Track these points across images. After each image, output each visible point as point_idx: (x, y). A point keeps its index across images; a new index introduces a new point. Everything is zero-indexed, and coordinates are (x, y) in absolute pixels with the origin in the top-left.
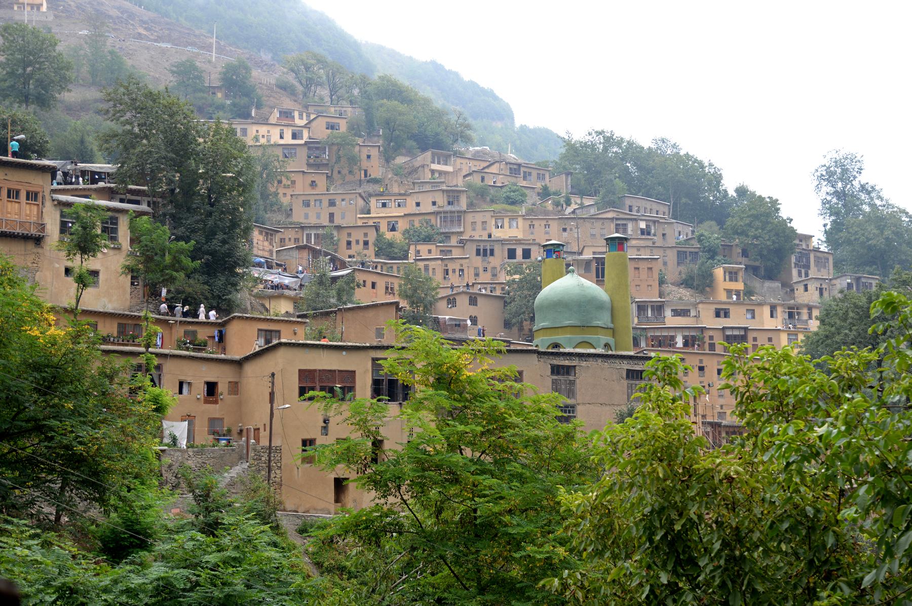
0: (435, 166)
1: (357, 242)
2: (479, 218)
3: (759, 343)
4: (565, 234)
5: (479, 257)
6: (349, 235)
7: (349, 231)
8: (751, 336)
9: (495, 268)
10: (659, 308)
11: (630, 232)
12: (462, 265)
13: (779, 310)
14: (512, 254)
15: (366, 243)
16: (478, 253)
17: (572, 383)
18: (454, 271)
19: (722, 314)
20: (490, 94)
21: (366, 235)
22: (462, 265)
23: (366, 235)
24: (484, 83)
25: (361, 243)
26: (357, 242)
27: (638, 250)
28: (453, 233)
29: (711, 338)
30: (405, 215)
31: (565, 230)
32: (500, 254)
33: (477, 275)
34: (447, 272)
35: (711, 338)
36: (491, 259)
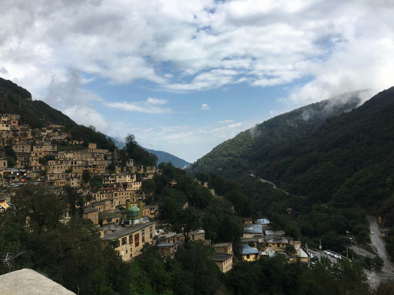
0: (42, 134)
1: (34, 159)
2: (62, 152)
3: (129, 185)
4: (82, 156)
6: (32, 158)
7: (32, 157)
8: (128, 183)
10: (108, 177)
13: (130, 176)
14: (72, 163)
15: (36, 160)
17: (144, 232)
20: (25, 90)
21: (36, 158)
23: (36, 158)
25: (35, 160)
26: (34, 159)
29: (121, 185)
33: (65, 168)
35: (121, 185)
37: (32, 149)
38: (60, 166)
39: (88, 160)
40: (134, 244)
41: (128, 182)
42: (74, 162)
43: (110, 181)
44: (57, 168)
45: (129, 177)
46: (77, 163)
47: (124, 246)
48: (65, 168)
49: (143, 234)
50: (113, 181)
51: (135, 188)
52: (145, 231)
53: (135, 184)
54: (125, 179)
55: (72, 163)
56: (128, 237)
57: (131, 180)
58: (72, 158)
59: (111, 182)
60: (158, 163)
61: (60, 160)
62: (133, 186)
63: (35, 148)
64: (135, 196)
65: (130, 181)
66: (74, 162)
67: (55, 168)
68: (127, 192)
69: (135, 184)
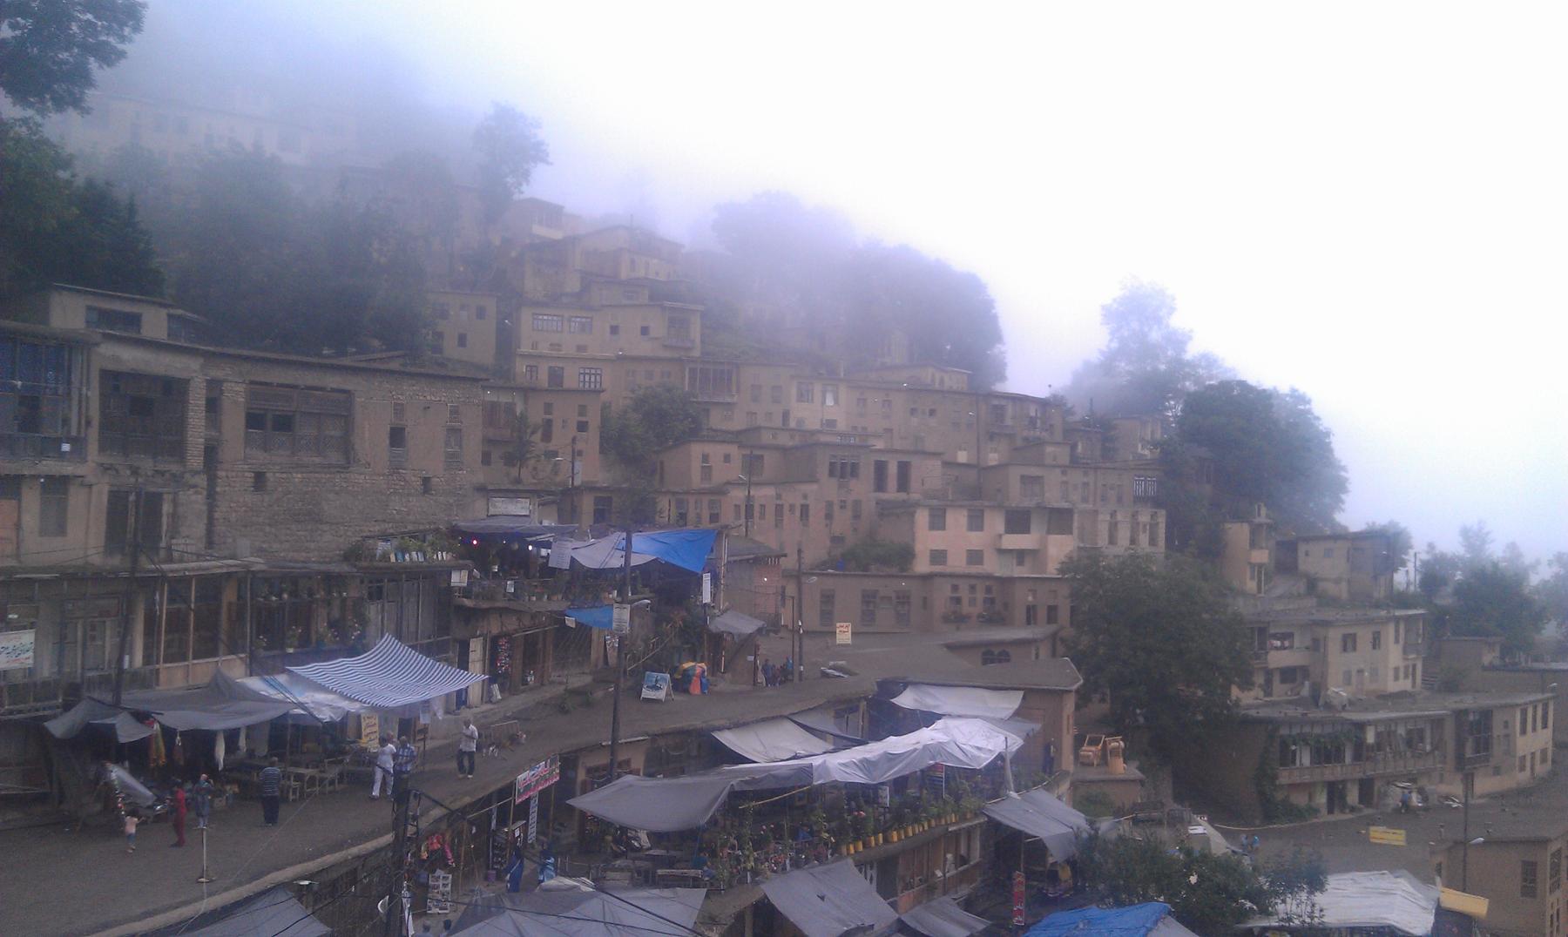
4: (915, 421)
5: (834, 482)
9: (857, 503)
11: (1009, 422)
12: (805, 497)
14: (881, 468)
15: (582, 427)
16: (831, 474)
18: (792, 508)
19: (1349, 644)
21: (582, 410)
22: (805, 497)
27: (1086, 474)
28: (718, 404)
30: (619, 358)
31: (913, 411)
32: (867, 471)
33: (829, 516)
34: (779, 509)
36: (853, 483)
38: (792, 497)
42: (893, 469)
44: (770, 510)
45: (1397, 641)
48: (829, 516)
55: (881, 468)
57: (1406, 677)
59: (1276, 679)
66: (893, 469)
67: (762, 516)
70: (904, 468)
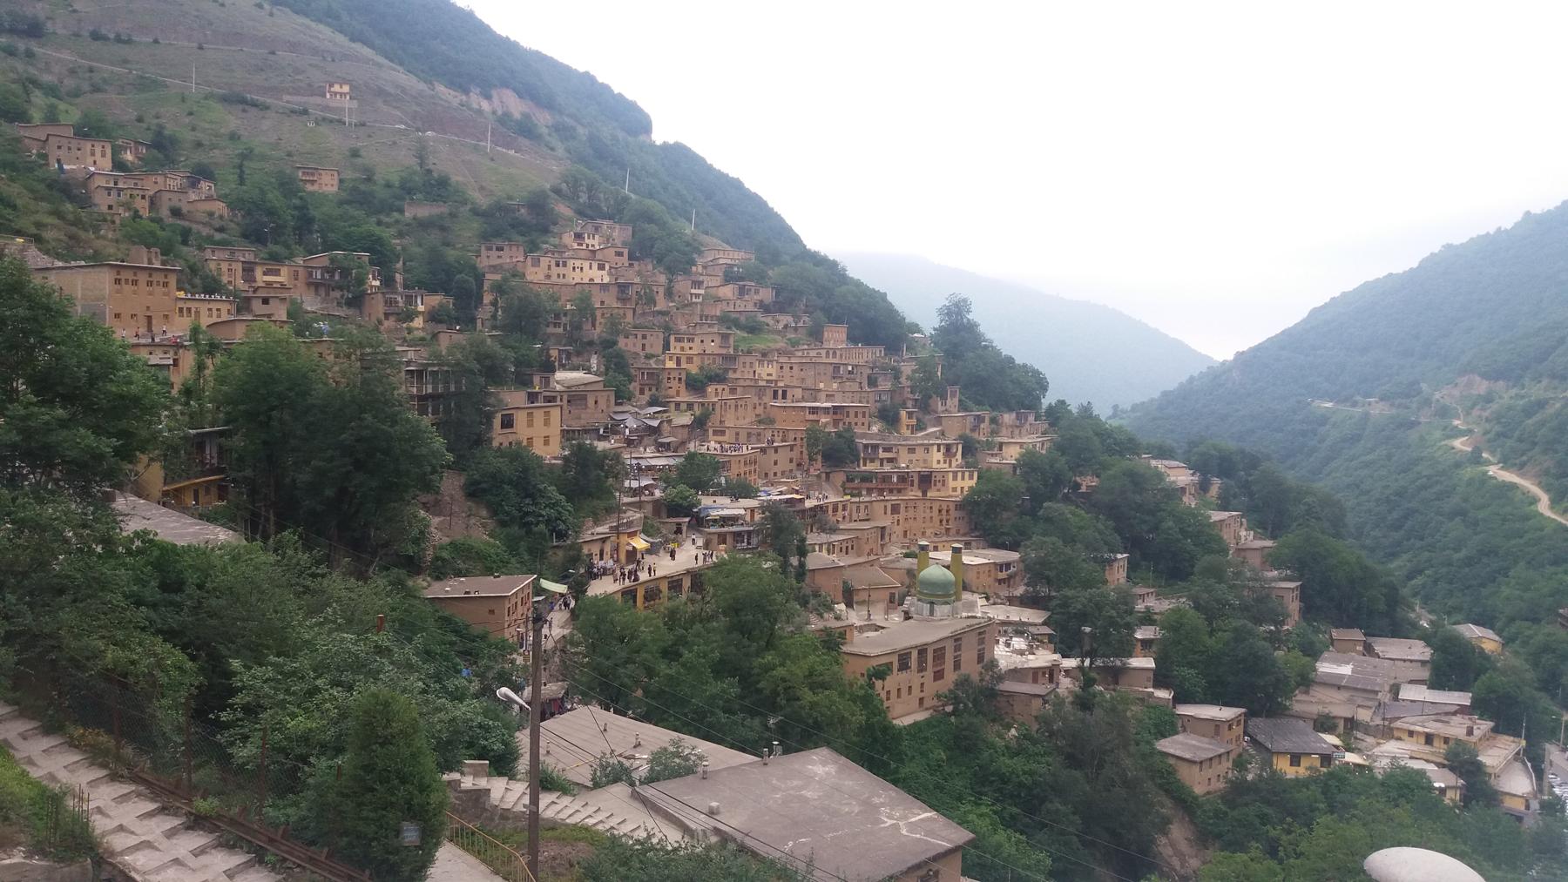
14: (775, 393)
20: (633, 107)
24: (630, 96)
32: (770, 393)
37: (666, 346)
39: (822, 386)
40: (929, 673)
41: (935, 465)
43: (882, 460)
46: (789, 395)
47: (904, 675)
49: (957, 648)
50: (890, 460)
51: (954, 489)
52: (964, 643)
53: (955, 478)
54: (927, 456)
55: (775, 393)
56: (915, 654)
58: (774, 377)
60: (1048, 400)
61: (742, 383)
62: (951, 484)
63: (675, 348)
64: (952, 517)
65: (942, 465)
68: (928, 504)
69: (955, 478)
70: (784, 393)
